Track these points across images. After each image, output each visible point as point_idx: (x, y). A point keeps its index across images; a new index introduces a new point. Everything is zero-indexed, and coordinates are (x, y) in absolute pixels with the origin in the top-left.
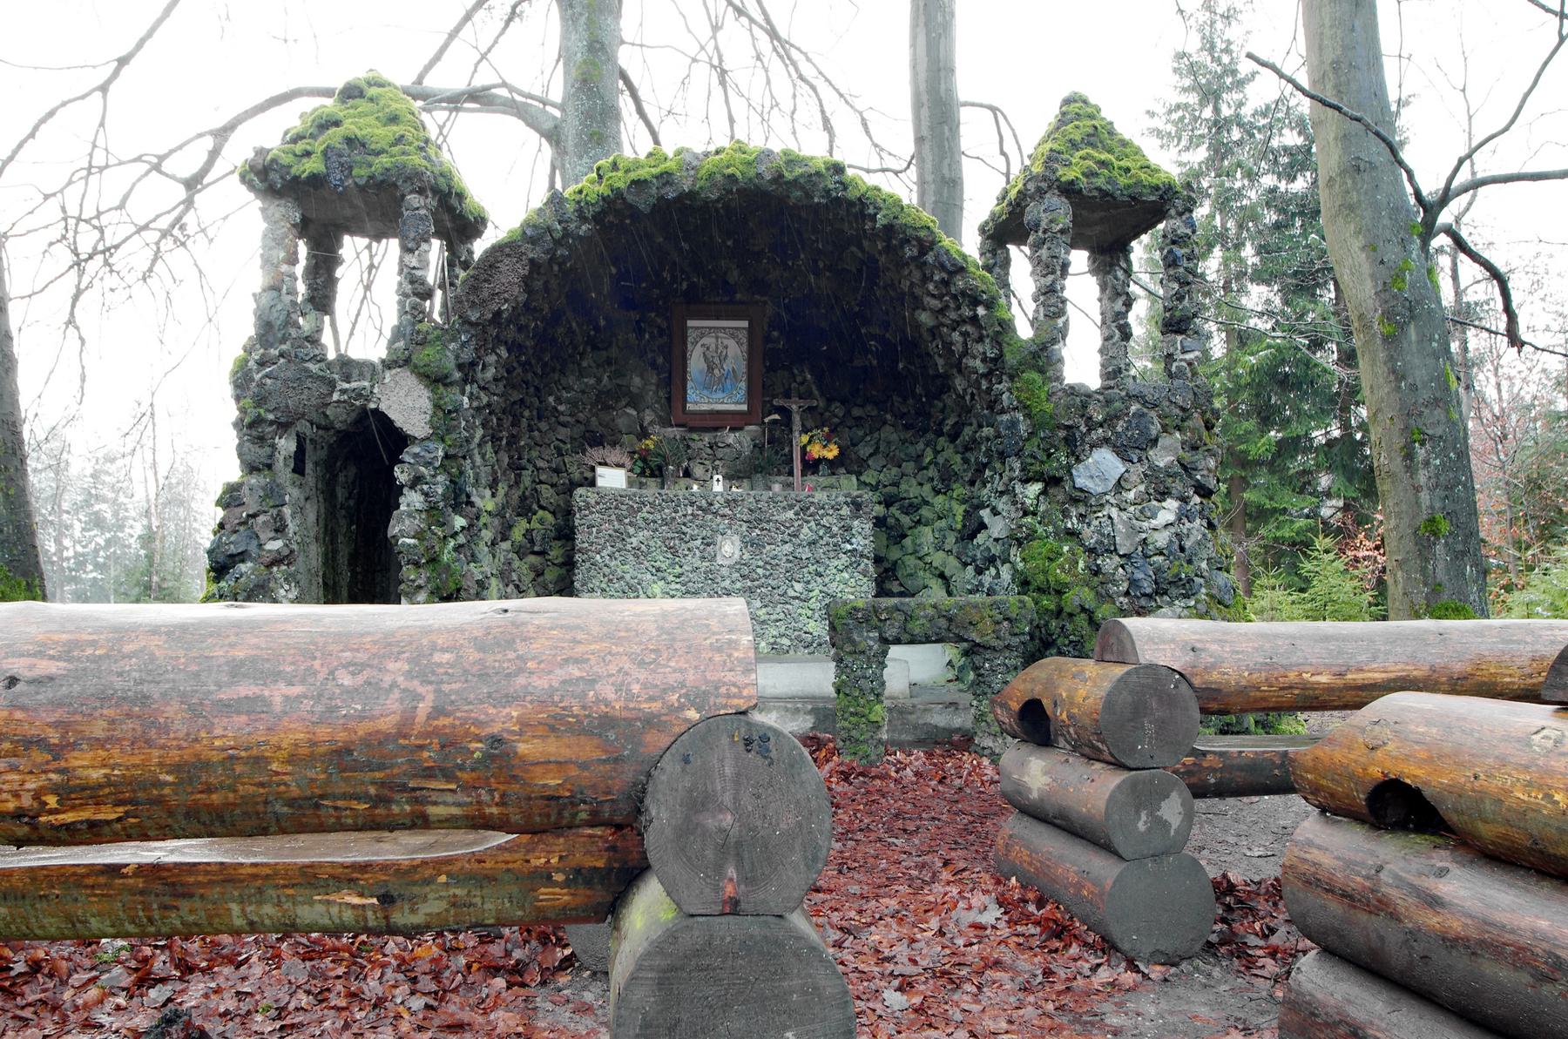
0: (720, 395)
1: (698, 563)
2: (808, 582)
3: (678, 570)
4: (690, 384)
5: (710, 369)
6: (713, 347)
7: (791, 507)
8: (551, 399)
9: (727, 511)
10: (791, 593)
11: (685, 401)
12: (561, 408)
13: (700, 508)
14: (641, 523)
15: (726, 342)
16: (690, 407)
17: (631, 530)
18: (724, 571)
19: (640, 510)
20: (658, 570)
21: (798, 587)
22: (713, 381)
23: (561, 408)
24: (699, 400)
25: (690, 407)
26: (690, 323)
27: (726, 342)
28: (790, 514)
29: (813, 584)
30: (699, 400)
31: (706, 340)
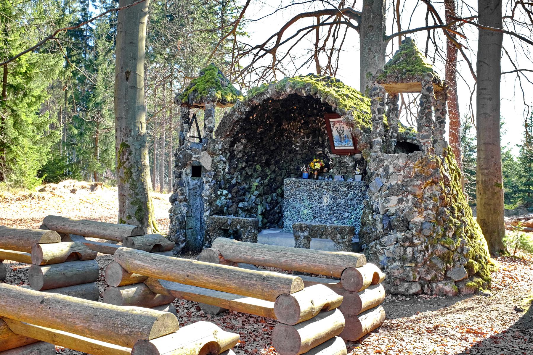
0: (345, 144)
1: (316, 204)
2: (351, 213)
3: (311, 206)
4: (334, 140)
5: (340, 135)
6: (339, 128)
7: (346, 186)
8: (293, 146)
9: (326, 187)
10: (344, 216)
11: (334, 146)
12: (298, 149)
13: (318, 186)
14: (301, 190)
15: (343, 126)
16: (336, 148)
17: (298, 192)
18: (325, 207)
19: (301, 186)
20: (305, 206)
21: (347, 214)
22: (342, 139)
23: (298, 149)
24: (338, 146)
25: (336, 148)
26: (330, 120)
27: (343, 126)
28: (345, 189)
29: (352, 213)
30: (338, 146)
31: (336, 125)
